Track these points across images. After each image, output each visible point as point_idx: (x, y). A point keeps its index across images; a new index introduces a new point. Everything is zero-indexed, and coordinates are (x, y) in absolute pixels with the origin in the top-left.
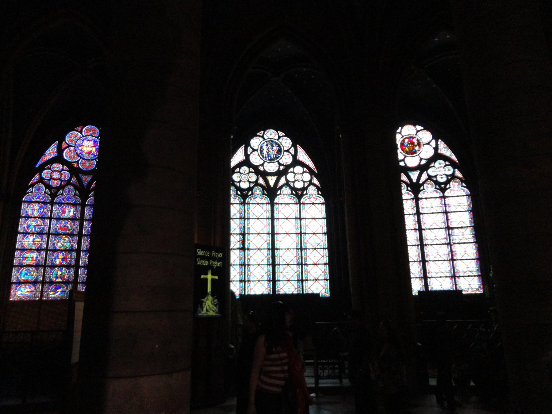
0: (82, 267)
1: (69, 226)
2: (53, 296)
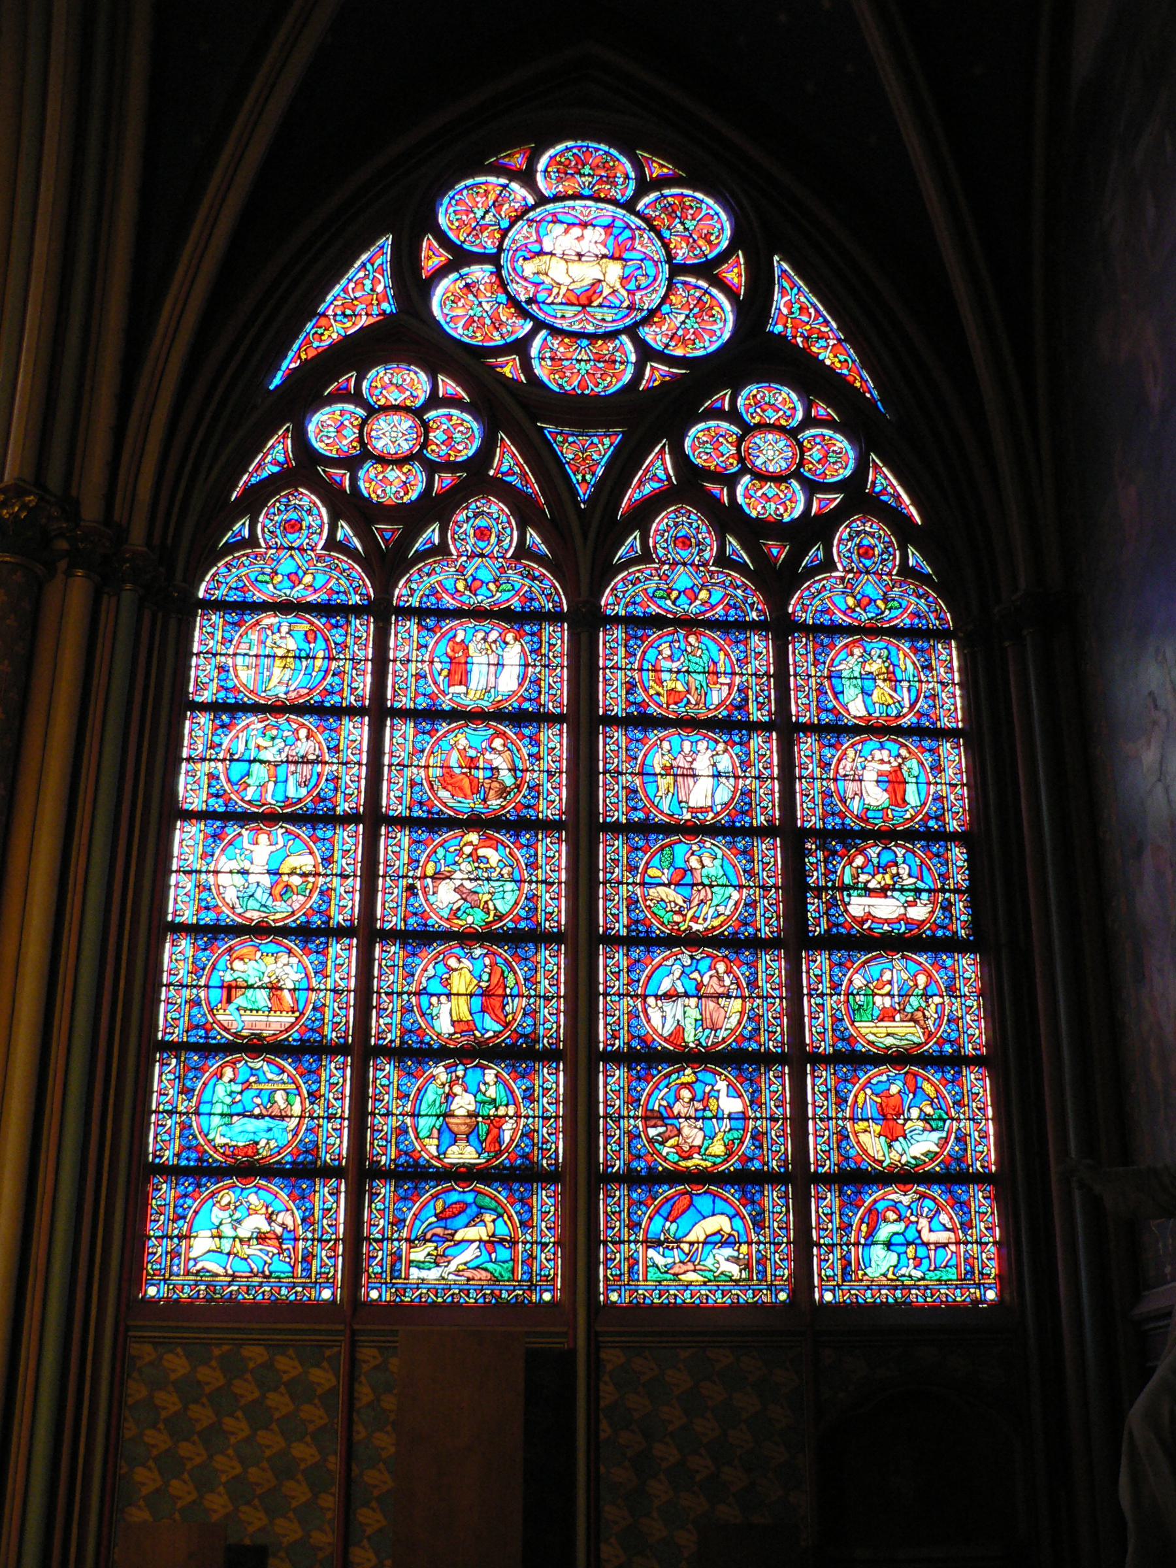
1: (498, 761)
2: (433, 1274)
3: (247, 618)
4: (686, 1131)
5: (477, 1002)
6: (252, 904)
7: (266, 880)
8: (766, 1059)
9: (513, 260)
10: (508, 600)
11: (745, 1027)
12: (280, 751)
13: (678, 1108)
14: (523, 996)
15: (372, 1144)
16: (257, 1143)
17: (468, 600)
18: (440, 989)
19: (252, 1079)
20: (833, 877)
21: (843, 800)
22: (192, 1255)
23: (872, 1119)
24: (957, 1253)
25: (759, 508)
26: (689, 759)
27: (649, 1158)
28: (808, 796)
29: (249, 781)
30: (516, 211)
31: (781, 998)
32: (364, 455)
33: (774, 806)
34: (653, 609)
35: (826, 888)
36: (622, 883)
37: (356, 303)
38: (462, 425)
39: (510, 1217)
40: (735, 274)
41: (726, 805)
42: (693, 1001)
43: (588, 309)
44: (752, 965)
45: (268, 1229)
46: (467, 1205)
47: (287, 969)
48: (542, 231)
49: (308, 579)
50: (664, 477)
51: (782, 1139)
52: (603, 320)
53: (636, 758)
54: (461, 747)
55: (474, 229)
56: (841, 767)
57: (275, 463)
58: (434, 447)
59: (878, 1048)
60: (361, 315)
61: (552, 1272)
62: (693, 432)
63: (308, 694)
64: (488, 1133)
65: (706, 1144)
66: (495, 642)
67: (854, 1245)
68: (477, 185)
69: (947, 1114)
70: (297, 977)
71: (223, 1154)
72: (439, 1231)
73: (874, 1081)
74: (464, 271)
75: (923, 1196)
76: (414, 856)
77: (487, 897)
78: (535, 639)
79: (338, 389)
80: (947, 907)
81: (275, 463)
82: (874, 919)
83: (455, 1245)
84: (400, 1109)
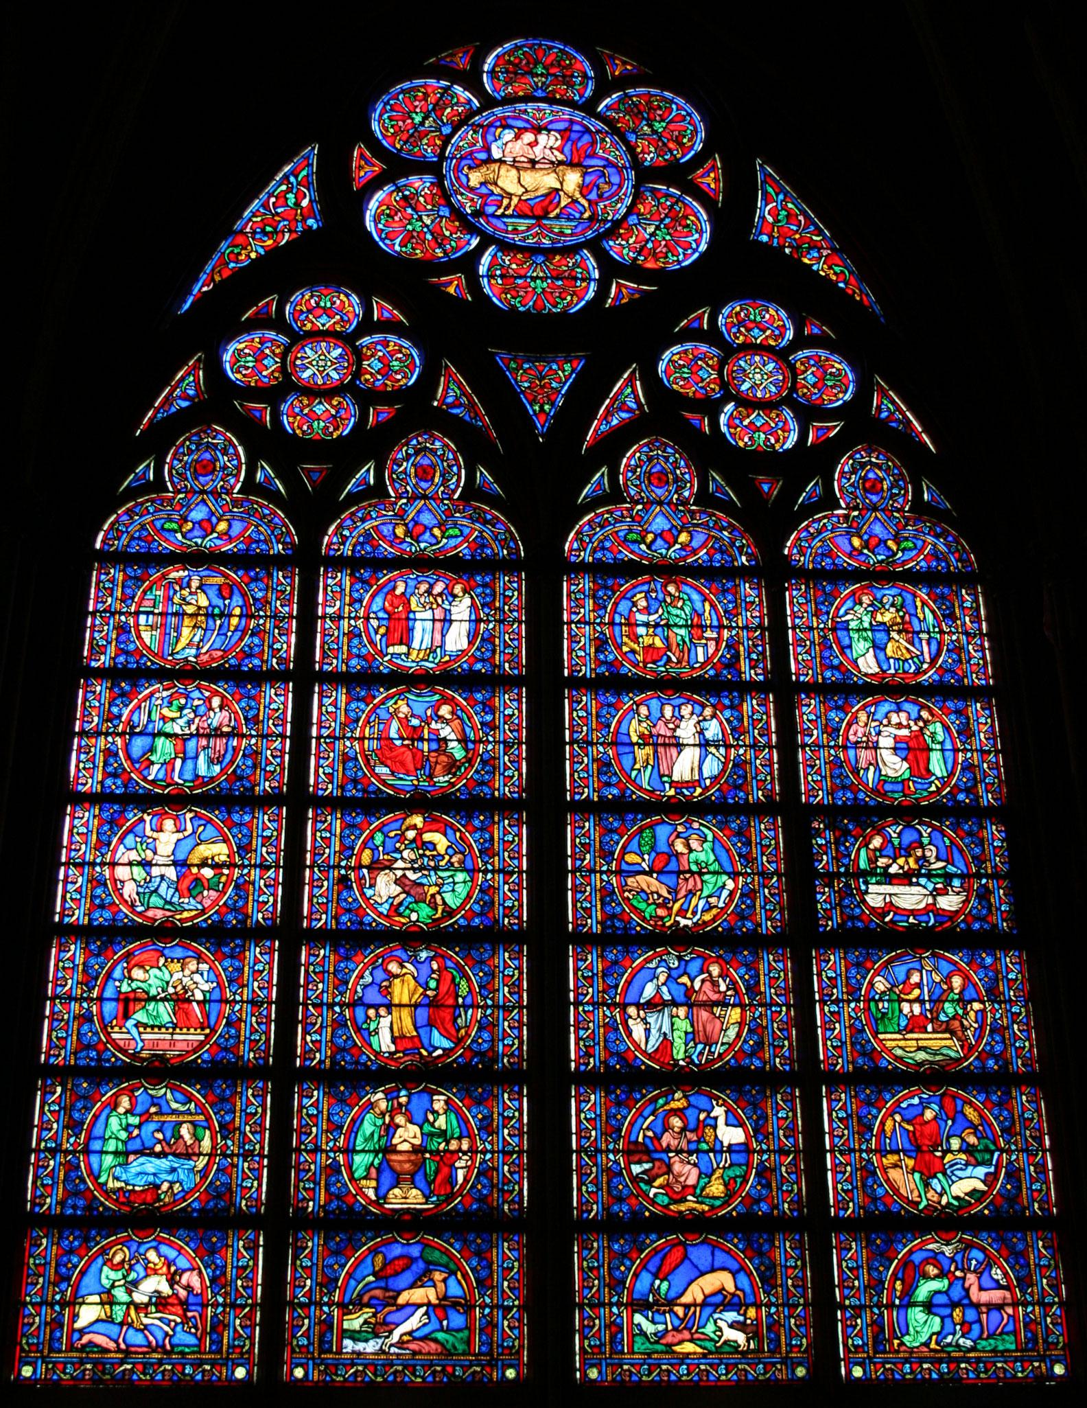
0: (590, 1080)
1: (446, 732)
2: (371, 1347)
3: (151, 571)
4: (677, 1167)
5: (422, 1014)
6: (155, 900)
7: (171, 873)
8: (770, 1080)
9: (458, 169)
10: (456, 547)
11: (745, 1042)
12: (189, 723)
13: (667, 1139)
14: (479, 1006)
15: (297, 1187)
16: (158, 1187)
17: (410, 547)
18: (379, 999)
19: (153, 1110)
20: (846, 861)
21: (855, 771)
22: (77, 1325)
23: (904, 1150)
24: (1014, 1317)
25: (746, 439)
26: (671, 726)
27: (633, 1201)
28: (812, 767)
29: (153, 758)
30: (459, 114)
31: (788, 1007)
32: (286, 386)
33: (773, 779)
34: (626, 555)
35: (838, 875)
36: (595, 872)
37: (277, 218)
38: (400, 352)
39: (465, 1276)
40: (710, 180)
41: (715, 779)
42: (682, 1011)
43: (545, 222)
44: (752, 967)
45: (170, 1292)
46: (413, 1260)
47: (197, 977)
48: (490, 138)
49: (222, 526)
50: (634, 406)
51: (793, 1176)
52: (561, 234)
53: (609, 726)
54: (401, 715)
55: (412, 135)
56: (851, 732)
57: (185, 397)
58: (368, 377)
59: (907, 1065)
60: (283, 232)
61: (516, 1343)
62: (666, 355)
63: (222, 657)
64: (437, 1172)
65: (702, 1183)
66: (440, 595)
67: (886, 1307)
68: (416, 89)
69: (995, 1143)
70: (206, 987)
71: (117, 1200)
72: (378, 1293)
73: (904, 1105)
74: (402, 181)
75: (970, 1246)
76: (347, 842)
77: (433, 890)
78: (488, 591)
79: (256, 313)
80: (984, 895)
81: (185, 397)
82: (898, 910)
83: (398, 1310)
84: (331, 1144)
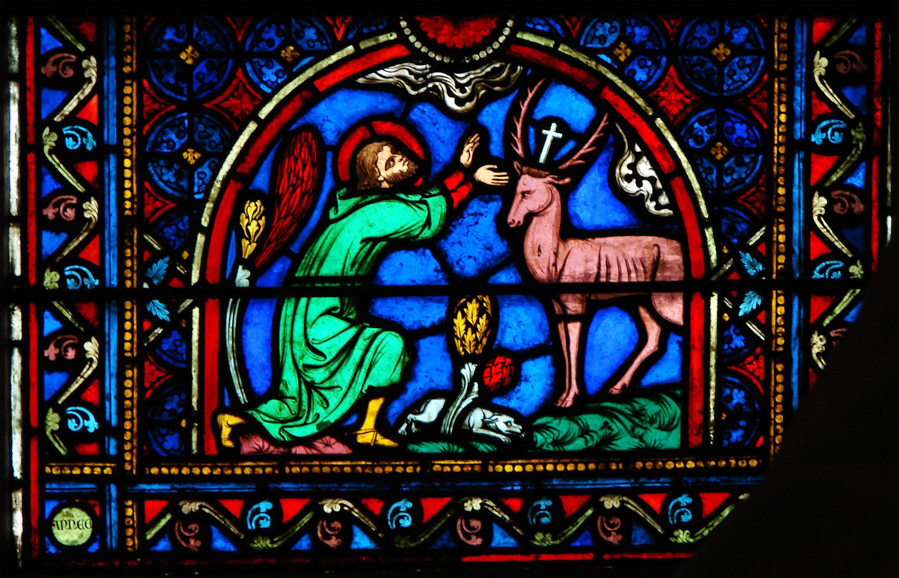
75: (545, 72)
